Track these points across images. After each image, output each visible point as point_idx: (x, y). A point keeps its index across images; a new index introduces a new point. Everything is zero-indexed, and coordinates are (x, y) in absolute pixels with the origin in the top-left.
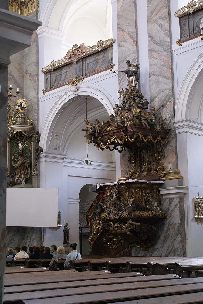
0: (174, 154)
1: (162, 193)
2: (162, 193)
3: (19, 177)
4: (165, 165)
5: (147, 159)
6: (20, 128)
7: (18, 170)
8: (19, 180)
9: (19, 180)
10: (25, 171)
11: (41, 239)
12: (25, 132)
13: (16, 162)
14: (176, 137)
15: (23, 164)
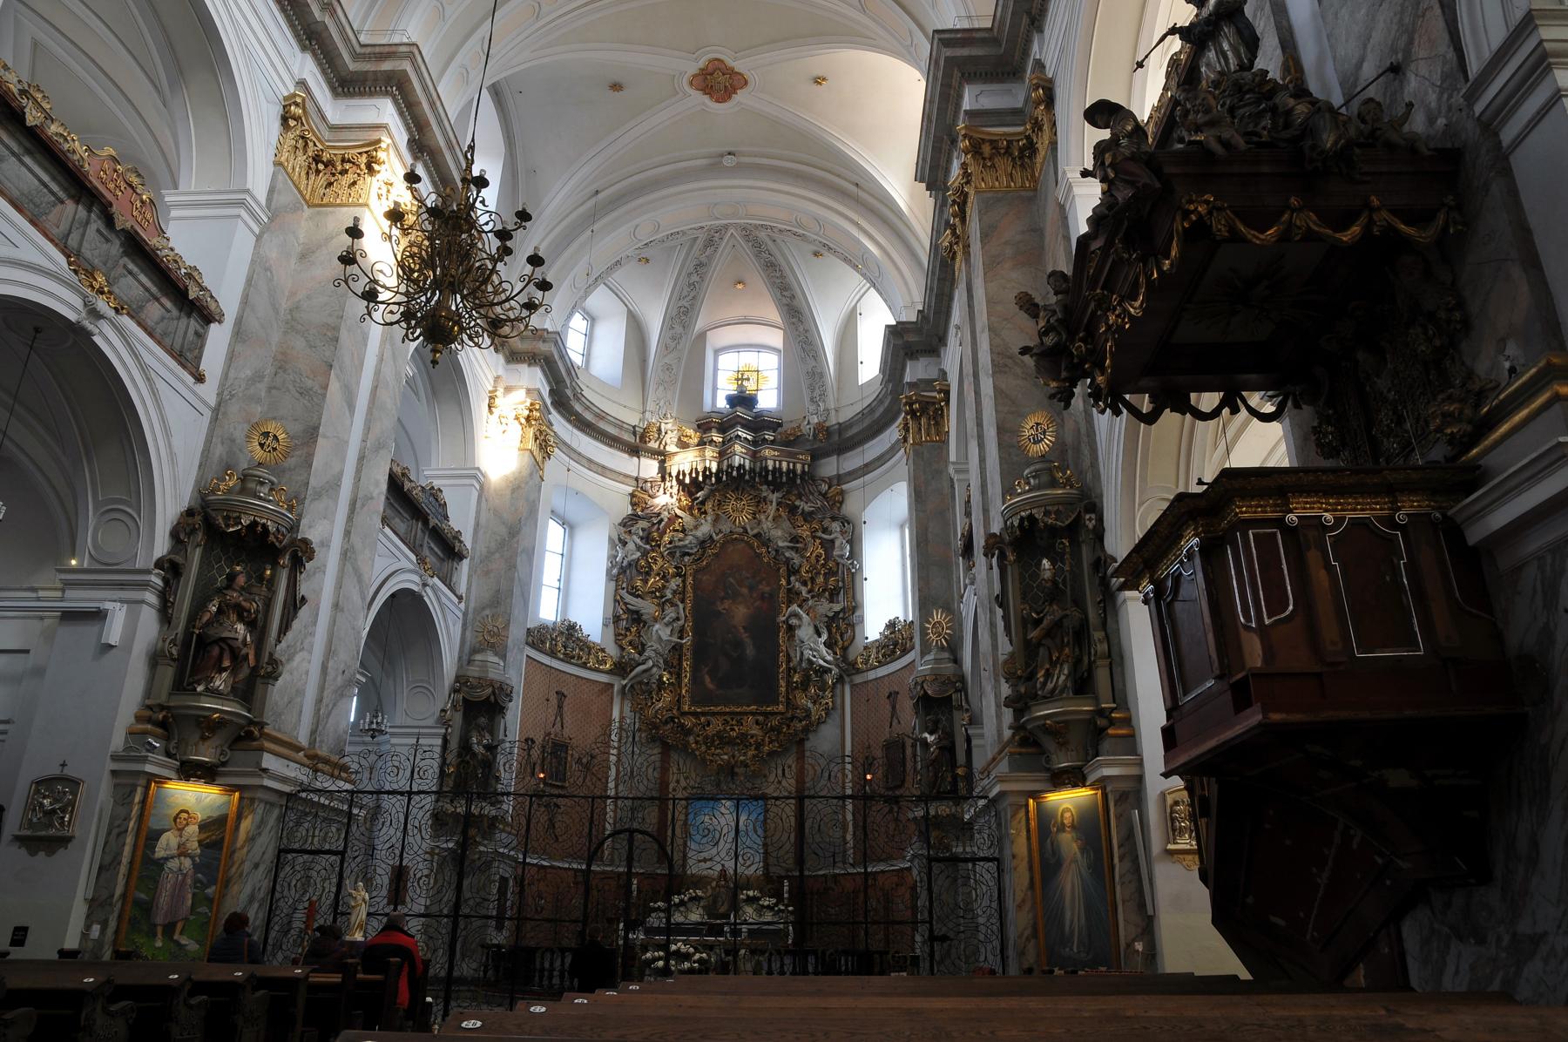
0: (1516, 272)
1: (1475, 534)
2: (1475, 534)
3: (1048, 675)
4: (1481, 368)
5: (1391, 396)
6: (1031, 503)
7: (1042, 650)
8: (1050, 686)
9: (1050, 686)
10: (1067, 650)
11: (1142, 906)
12: (1047, 513)
13: (1038, 622)
14: (1507, 172)
15: (1058, 624)
